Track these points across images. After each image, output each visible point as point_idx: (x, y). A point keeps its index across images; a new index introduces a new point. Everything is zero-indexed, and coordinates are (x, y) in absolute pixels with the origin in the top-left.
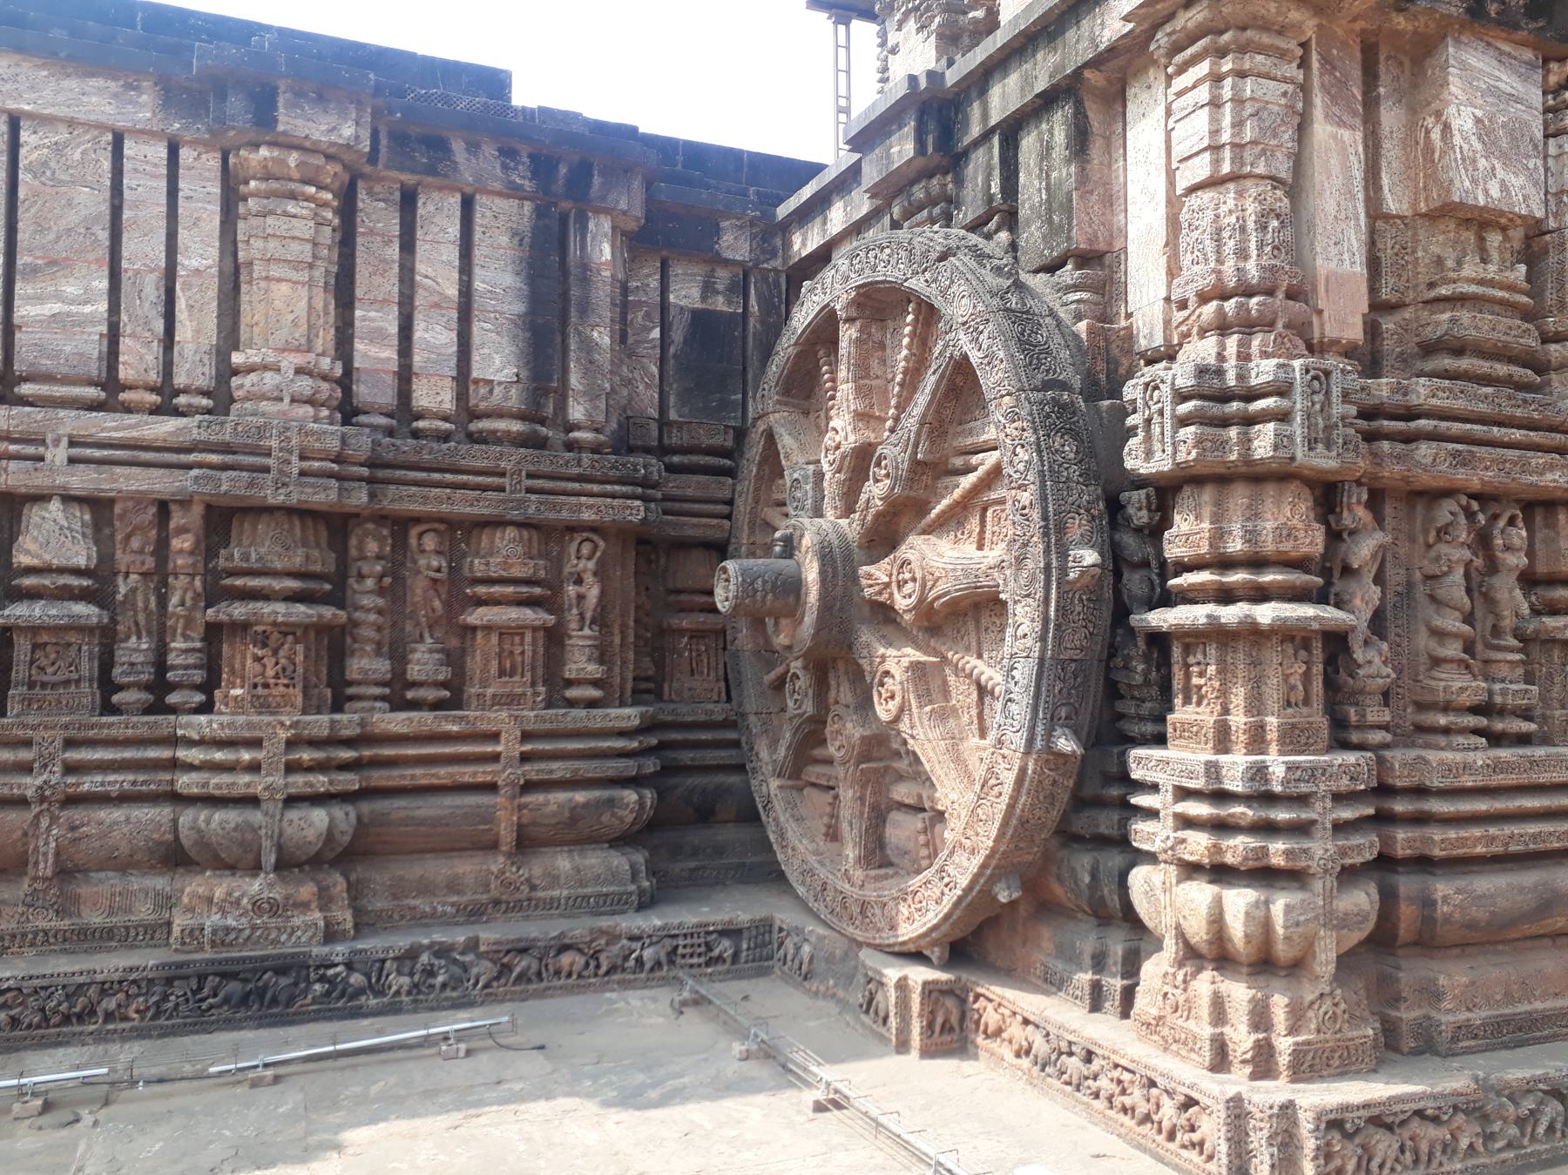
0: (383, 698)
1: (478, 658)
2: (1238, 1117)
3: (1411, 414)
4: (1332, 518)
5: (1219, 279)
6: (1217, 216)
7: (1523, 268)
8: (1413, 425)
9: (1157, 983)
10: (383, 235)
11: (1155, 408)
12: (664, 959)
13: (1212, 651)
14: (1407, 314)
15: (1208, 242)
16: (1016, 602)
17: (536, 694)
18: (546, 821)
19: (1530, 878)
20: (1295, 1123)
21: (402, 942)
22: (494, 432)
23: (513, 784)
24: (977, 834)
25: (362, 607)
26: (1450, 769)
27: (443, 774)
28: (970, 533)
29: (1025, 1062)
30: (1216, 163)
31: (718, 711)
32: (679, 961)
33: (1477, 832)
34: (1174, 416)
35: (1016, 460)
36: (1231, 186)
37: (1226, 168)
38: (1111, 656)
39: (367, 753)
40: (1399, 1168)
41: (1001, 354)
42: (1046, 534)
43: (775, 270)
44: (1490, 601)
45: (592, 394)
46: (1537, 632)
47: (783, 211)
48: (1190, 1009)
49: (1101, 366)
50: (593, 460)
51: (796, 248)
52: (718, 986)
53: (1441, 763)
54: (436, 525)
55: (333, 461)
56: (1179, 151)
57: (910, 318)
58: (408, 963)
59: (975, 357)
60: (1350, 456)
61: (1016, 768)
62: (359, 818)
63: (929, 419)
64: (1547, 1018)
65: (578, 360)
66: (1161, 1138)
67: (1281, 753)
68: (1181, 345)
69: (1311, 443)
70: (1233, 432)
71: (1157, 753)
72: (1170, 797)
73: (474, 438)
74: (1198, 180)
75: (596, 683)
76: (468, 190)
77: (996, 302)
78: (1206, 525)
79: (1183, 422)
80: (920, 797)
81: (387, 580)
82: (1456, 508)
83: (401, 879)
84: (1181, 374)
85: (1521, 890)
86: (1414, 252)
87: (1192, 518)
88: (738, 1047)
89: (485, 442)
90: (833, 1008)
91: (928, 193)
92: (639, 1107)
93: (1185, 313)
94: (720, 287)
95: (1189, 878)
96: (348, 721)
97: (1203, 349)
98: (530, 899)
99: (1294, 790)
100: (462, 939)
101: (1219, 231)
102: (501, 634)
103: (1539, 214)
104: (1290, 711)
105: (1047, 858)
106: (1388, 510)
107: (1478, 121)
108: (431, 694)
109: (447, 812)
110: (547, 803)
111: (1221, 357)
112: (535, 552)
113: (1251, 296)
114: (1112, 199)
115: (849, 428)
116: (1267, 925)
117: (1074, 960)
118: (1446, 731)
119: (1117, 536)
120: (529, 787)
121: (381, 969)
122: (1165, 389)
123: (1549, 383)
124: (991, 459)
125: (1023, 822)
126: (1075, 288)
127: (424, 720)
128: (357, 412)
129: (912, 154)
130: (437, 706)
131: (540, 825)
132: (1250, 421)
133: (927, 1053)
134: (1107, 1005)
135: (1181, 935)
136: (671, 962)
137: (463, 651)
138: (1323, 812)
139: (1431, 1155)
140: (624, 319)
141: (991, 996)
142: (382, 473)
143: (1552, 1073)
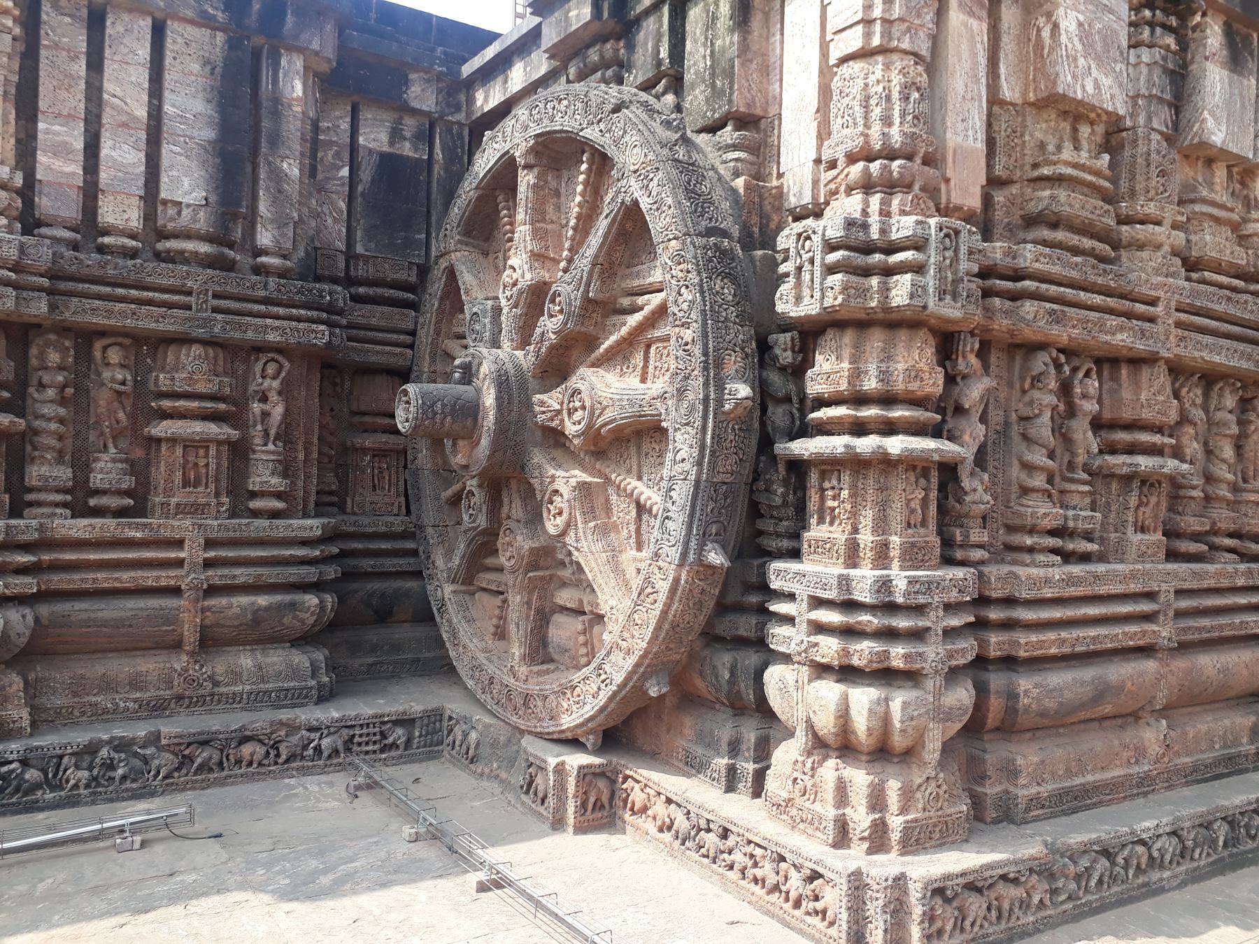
0: (65, 505)
1: (162, 469)
2: (857, 888)
3: (1018, 276)
4: (948, 363)
5: (867, 142)
6: (866, 85)
7: (1107, 157)
8: (1019, 285)
9: (788, 770)
10: (69, 51)
11: (806, 257)
12: (341, 748)
13: (846, 478)
14: (1014, 189)
15: (857, 108)
16: (676, 430)
17: (220, 504)
18: (229, 623)
19: (1088, 673)
20: (906, 892)
21: (80, 737)
22: (182, 252)
23: (196, 588)
24: (633, 637)
25: (43, 416)
26: (1035, 583)
27: (126, 578)
28: (635, 368)
29: (667, 837)
30: (868, 35)
31: (398, 523)
32: (355, 748)
33: (1051, 635)
34: (823, 264)
35: (680, 299)
36: (880, 58)
37: (876, 41)
38: (755, 480)
39: (46, 557)
40: (986, 925)
41: (670, 201)
42: (706, 369)
43: (458, 123)
44: (1066, 439)
45: (280, 222)
46: (1100, 467)
47: (467, 69)
48: (816, 793)
49: (755, 219)
50: (279, 284)
51: (479, 103)
52: (391, 771)
53: (1029, 577)
54: (120, 340)
55: (9, 270)
56: (833, 24)
57: (584, 167)
58: (87, 758)
59: (644, 204)
60: (971, 308)
61: (671, 579)
62: (37, 620)
63: (601, 260)
64: (1096, 788)
65: (267, 189)
66: (788, 906)
67: (902, 568)
68: (827, 203)
69: (941, 294)
70: (874, 281)
71: (793, 566)
72: (805, 605)
73: (159, 256)
74: (850, 51)
75: (279, 496)
76: (159, 15)
77: (665, 152)
78: (846, 365)
79: (831, 270)
80: (581, 601)
81: (70, 391)
82: (1048, 360)
83: (82, 677)
84: (831, 225)
85: (1082, 683)
86: (1022, 135)
87: (834, 358)
88: (408, 830)
89: (173, 261)
90: (495, 787)
91: (602, 56)
92: (313, 897)
93: (834, 172)
94: (408, 134)
95: (819, 677)
96: (27, 527)
97: (850, 205)
98: (212, 695)
99: (913, 602)
100: (143, 733)
101: (868, 98)
102: (185, 447)
103: (1121, 112)
104: (910, 531)
105: (692, 655)
106: (993, 359)
107: (1080, 24)
108: (114, 502)
109: (130, 614)
110: (230, 606)
111: (865, 213)
112: (220, 369)
113: (893, 159)
114: (769, 69)
115: (526, 267)
116: (886, 719)
117: (711, 744)
118: (1031, 550)
119: (764, 374)
120: (212, 590)
121: (59, 764)
122: (817, 239)
123: (1118, 258)
124: (655, 300)
125: (674, 626)
126: (735, 147)
127: (106, 526)
128: (39, 224)
129: (588, 17)
130: (121, 513)
131: (223, 626)
132: (888, 272)
133: (580, 829)
134: (740, 786)
135: (810, 727)
136: (348, 750)
137: (148, 463)
138: (936, 621)
139: (1011, 910)
140: (314, 155)
141: (638, 778)
142: (62, 285)
143: (1104, 836)
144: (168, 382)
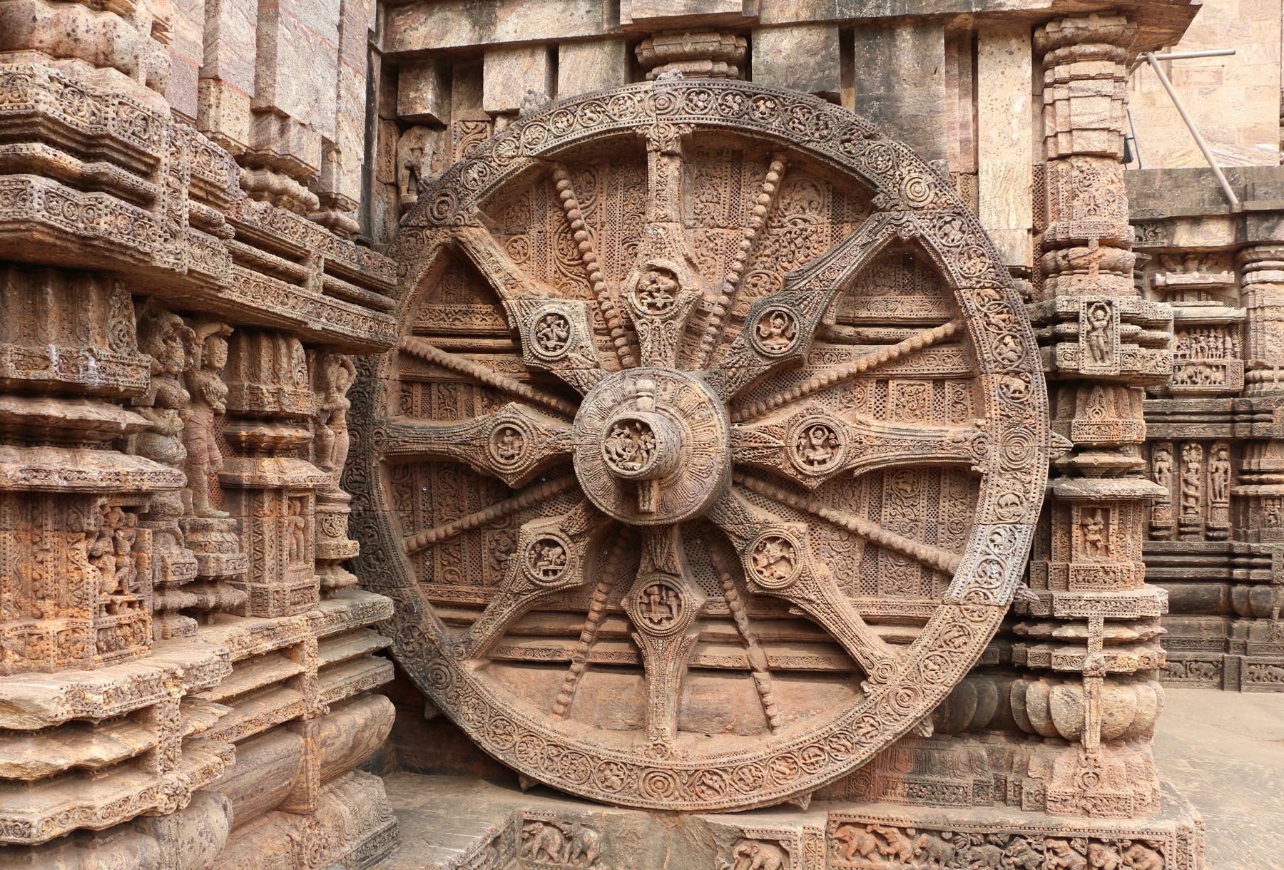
79: (1126, 339)
144: (271, 400)
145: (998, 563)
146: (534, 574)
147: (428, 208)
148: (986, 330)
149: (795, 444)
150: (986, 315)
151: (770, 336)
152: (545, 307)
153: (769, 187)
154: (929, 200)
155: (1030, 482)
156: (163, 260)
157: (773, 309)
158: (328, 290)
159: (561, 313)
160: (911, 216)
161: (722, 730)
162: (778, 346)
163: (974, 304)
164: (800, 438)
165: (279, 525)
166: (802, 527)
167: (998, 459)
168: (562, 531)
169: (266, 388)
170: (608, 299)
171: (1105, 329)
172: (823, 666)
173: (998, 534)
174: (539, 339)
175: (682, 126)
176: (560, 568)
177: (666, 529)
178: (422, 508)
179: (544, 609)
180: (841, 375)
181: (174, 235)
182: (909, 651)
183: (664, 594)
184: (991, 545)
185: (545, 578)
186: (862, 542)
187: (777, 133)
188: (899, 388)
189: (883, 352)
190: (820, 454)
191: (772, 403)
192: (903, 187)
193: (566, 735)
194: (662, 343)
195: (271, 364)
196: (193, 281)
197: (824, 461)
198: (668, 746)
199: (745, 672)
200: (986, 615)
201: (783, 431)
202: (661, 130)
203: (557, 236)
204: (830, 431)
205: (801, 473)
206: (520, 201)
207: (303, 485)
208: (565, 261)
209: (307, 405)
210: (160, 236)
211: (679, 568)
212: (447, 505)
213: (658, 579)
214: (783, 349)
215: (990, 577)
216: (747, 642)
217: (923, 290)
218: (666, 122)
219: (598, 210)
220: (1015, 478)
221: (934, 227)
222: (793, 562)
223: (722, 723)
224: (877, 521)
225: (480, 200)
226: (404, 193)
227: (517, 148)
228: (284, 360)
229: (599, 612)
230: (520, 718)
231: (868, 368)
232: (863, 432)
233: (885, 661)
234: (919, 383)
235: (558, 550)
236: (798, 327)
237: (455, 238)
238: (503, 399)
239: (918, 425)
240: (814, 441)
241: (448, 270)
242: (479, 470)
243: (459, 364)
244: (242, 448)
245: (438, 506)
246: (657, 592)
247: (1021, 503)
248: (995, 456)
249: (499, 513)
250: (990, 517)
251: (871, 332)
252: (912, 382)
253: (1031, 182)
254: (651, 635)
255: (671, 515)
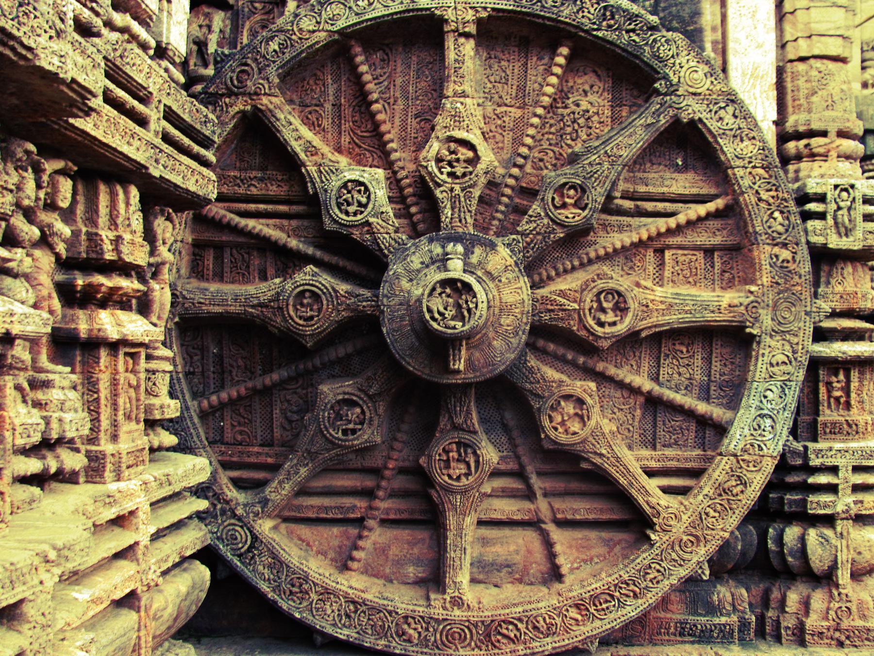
144: (110, 248)
145: (771, 417)
146: (333, 433)
147: (228, 76)
148: (757, 205)
149: (587, 307)
150: (757, 192)
151: (564, 206)
152: (346, 174)
153: (557, 70)
154: (706, 87)
155: (797, 344)
156: (47, 62)
157: (567, 180)
158: (167, 138)
159: (361, 179)
160: (690, 101)
161: (510, 580)
162: (572, 216)
163: (746, 182)
164: (592, 301)
165: (114, 383)
166: (593, 385)
167: (770, 322)
168: (360, 390)
169: (106, 235)
170: (403, 168)
171: (849, 209)
172: (605, 517)
173: (771, 390)
174: (339, 205)
175: (480, 9)
176: (359, 427)
177: (465, 387)
178: (212, 369)
179: (337, 467)
180: (625, 244)
181: (59, 34)
182: (691, 500)
183: (462, 451)
184: (764, 401)
185: (344, 438)
186: (641, 399)
187: (567, 20)
188: (674, 257)
189: (662, 224)
190: (610, 317)
191: (561, 268)
192: (682, 74)
193: (363, 591)
194: (462, 209)
195: (108, 210)
196: (71, 94)
197: (614, 324)
198: (464, 598)
199: (533, 524)
200: (760, 465)
201: (577, 295)
202: (459, 13)
203: (351, 110)
204: (619, 294)
205: (593, 334)
206: (315, 75)
207: (141, 340)
208: (359, 132)
209: (139, 256)
210: (46, 32)
211: (477, 426)
212: (239, 367)
213: (456, 436)
214: (577, 218)
215: (764, 430)
216: (535, 495)
217: (694, 169)
218: (464, 5)
219: (392, 87)
220: (784, 340)
221: (710, 111)
222: (586, 419)
223: (510, 573)
224: (656, 379)
225: (280, 71)
226: (192, 67)
227: (318, 23)
228: (122, 206)
229: (393, 469)
230: (317, 576)
231: (650, 238)
232: (649, 297)
233: (670, 510)
234: (691, 252)
235: (358, 410)
236: (590, 198)
237: (255, 107)
238: (297, 263)
239: (693, 291)
240: (605, 305)
241: (242, 139)
242: (276, 331)
243: (254, 228)
244: (76, 298)
245: (229, 368)
246: (455, 449)
247: (790, 362)
248: (767, 320)
249: (293, 374)
250: (763, 375)
251: (649, 206)
252: (686, 252)
253: (775, 80)
254: (448, 490)
255: (478, 374)
